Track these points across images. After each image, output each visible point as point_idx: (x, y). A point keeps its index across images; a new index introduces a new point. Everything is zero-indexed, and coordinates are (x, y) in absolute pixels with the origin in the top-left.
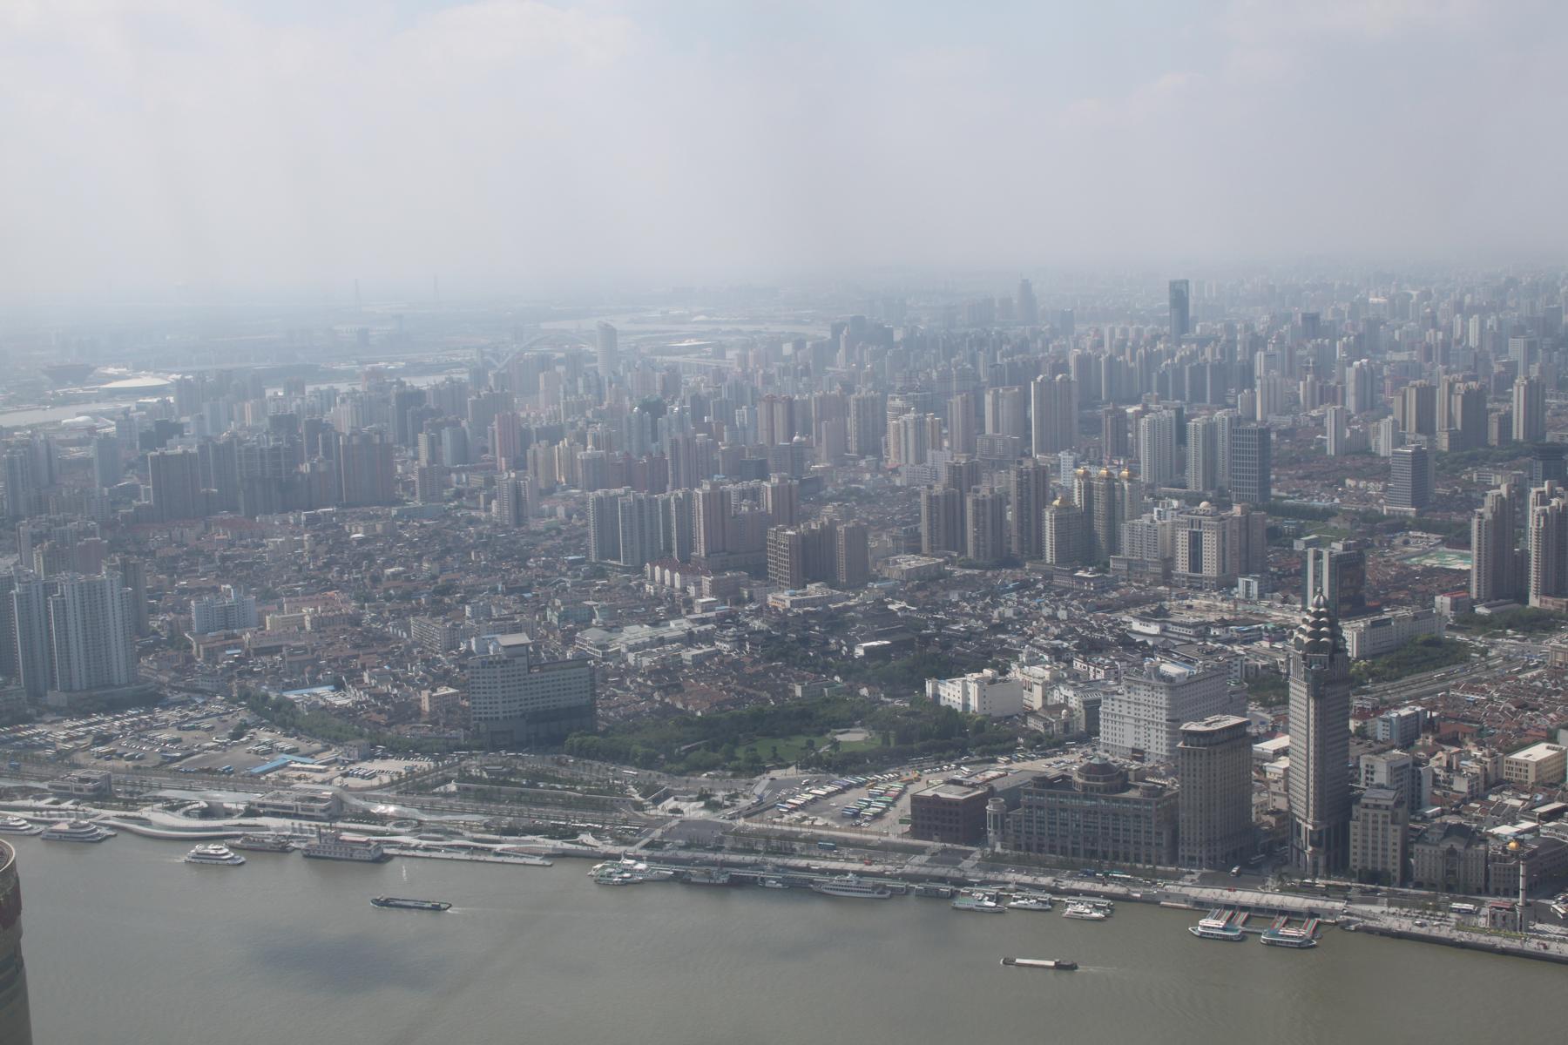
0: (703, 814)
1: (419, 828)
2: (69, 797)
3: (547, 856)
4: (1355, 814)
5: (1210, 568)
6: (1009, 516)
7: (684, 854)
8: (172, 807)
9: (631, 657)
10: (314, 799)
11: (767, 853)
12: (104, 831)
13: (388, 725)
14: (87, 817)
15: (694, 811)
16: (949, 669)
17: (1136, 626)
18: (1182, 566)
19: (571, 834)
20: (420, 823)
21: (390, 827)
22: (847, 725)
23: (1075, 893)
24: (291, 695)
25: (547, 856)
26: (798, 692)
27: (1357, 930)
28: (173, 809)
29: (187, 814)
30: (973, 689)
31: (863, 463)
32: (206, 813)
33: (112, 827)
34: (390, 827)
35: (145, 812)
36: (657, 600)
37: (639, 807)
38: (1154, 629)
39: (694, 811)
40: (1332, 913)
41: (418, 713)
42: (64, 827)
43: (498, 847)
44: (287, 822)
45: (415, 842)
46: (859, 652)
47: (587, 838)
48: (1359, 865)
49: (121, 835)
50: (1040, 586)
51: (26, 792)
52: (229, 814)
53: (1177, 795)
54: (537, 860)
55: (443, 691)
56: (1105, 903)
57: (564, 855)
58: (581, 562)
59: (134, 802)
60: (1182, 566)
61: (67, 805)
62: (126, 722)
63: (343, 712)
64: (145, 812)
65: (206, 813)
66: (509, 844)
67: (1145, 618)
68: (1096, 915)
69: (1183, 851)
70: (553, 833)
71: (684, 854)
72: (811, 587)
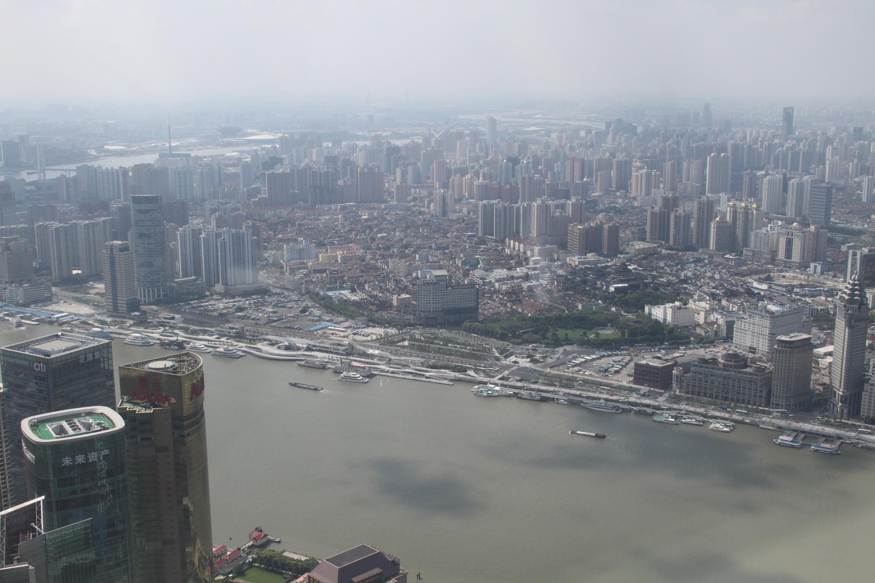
0: (528, 365)
1: (389, 362)
2: (224, 336)
3: (451, 380)
4: (865, 388)
5: (796, 257)
6: (693, 224)
7: (519, 384)
8: (272, 344)
9: (497, 285)
10: (339, 345)
11: (560, 386)
12: (240, 353)
13: (377, 311)
14: (232, 346)
15: (524, 363)
16: (657, 301)
17: (755, 284)
18: (781, 255)
19: (463, 370)
20: (390, 359)
21: (375, 361)
22: (604, 325)
23: (716, 418)
24: (330, 293)
25: (451, 380)
26: (580, 307)
27: (862, 447)
28: (272, 345)
29: (279, 348)
30: (669, 312)
31: (618, 194)
33: (244, 351)
34: (375, 361)
35: (259, 345)
36: (511, 257)
37: (497, 359)
38: (765, 287)
39: (524, 363)
40: (849, 438)
41: (391, 306)
42: (221, 350)
43: (428, 374)
44: (326, 355)
45: (387, 369)
46: (612, 289)
47: (471, 373)
48: (865, 414)
49: (248, 356)
50: (706, 261)
51: (205, 332)
52: (299, 349)
53: (772, 372)
54: (446, 382)
55: (403, 296)
56: (730, 423)
57: (460, 380)
58: (474, 236)
59: (254, 340)
60: (781, 255)
61: (223, 339)
62: (252, 302)
63: (356, 304)
64: (259, 345)
65: (288, 348)
66: (433, 373)
67: (760, 281)
68: (725, 429)
69: (773, 400)
70: (455, 369)
71: (519, 384)
72: (589, 255)
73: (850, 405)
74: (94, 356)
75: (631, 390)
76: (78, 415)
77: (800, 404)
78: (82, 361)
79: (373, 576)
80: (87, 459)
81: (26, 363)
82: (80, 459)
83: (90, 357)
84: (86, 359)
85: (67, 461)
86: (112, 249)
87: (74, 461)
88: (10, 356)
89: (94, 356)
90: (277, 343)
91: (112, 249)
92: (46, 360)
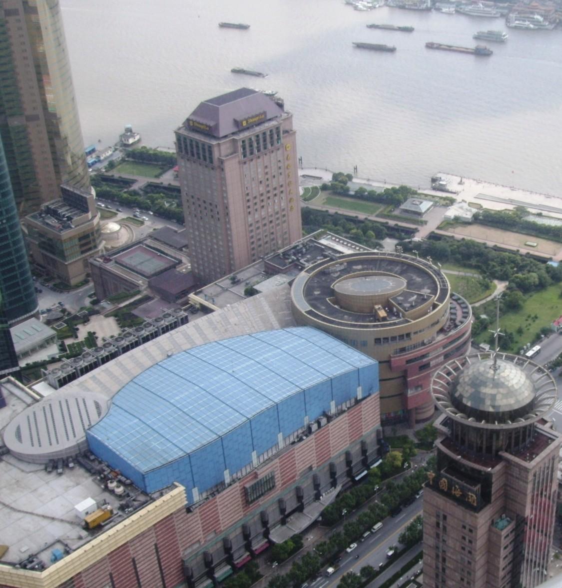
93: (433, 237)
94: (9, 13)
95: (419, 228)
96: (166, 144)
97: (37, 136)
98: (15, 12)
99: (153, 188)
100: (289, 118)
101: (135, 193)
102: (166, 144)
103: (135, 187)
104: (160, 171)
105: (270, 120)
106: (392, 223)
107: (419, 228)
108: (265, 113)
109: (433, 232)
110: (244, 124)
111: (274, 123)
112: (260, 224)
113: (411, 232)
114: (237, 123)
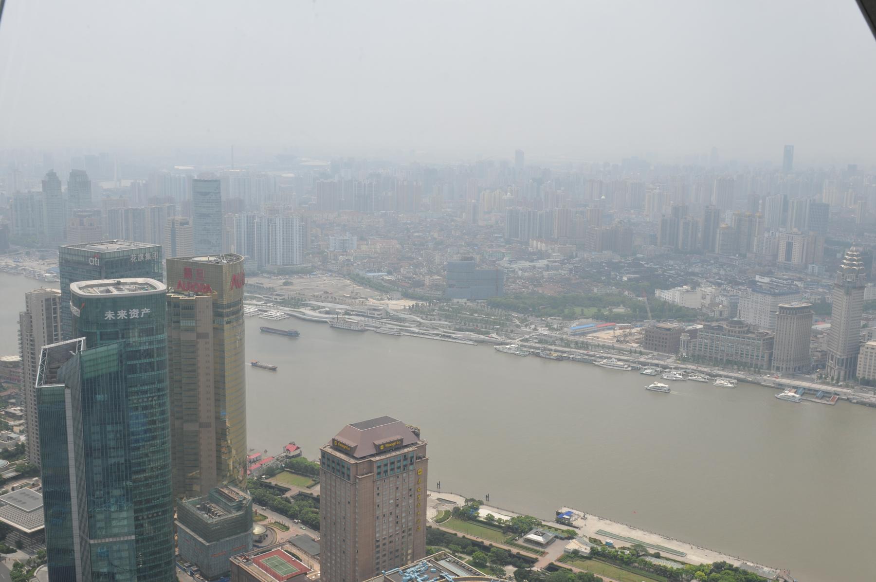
0: (546, 333)
1: (420, 325)
2: (271, 301)
3: (476, 341)
4: (861, 352)
5: (796, 259)
6: (699, 235)
7: (538, 345)
8: (314, 309)
9: (520, 272)
10: (375, 310)
11: (576, 348)
13: (410, 288)
15: (543, 331)
16: (667, 287)
17: (758, 278)
18: (781, 258)
19: (487, 334)
20: (421, 323)
21: (407, 324)
22: (617, 305)
23: (720, 376)
24: (370, 275)
25: (476, 341)
26: (595, 290)
27: (857, 403)
29: (320, 312)
30: (677, 294)
31: (632, 211)
32: (327, 313)
34: (407, 324)
35: (302, 310)
36: (534, 254)
37: (518, 326)
38: (766, 280)
39: (543, 331)
40: (845, 394)
41: (423, 285)
43: (454, 336)
44: (363, 319)
45: (417, 330)
46: (625, 279)
47: (494, 335)
48: (861, 376)
50: (712, 262)
51: (254, 298)
52: (338, 313)
53: (773, 338)
54: (471, 343)
55: (436, 277)
56: (735, 381)
57: (482, 342)
58: (501, 237)
60: (781, 258)
61: (271, 304)
63: (390, 282)
64: (302, 310)
65: (327, 313)
66: (459, 335)
67: (763, 275)
68: (730, 385)
69: (774, 364)
70: (479, 332)
71: (538, 345)
72: (605, 252)
73: (846, 368)
74: (145, 257)
75: (641, 353)
76: (125, 284)
77: (799, 369)
78: (133, 260)
79: (394, 441)
80: (128, 315)
81: (82, 259)
82: (122, 314)
83: (141, 258)
84: (137, 258)
85: (110, 315)
86: (173, 223)
87: (116, 316)
88: (68, 254)
89: (145, 257)
90: (319, 307)
91: (173, 223)
92: (100, 256)
93: (551, 568)
94: (199, 336)
95: (540, 558)
96: (313, 457)
97: (207, 441)
98: (205, 336)
99: (302, 496)
100: (424, 447)
101: (287, 500)
102: (313, 457)
103: (288, 495)
104: (310, 482)
105: (407, 446)
106: (514, 551)
107: (540, 558)
108: (401, 440)
109: (552, 564)
110: (382, 448)
111: (410, 449)
112: (387, 541)
113: (533, 561)
114: (377, 447)
